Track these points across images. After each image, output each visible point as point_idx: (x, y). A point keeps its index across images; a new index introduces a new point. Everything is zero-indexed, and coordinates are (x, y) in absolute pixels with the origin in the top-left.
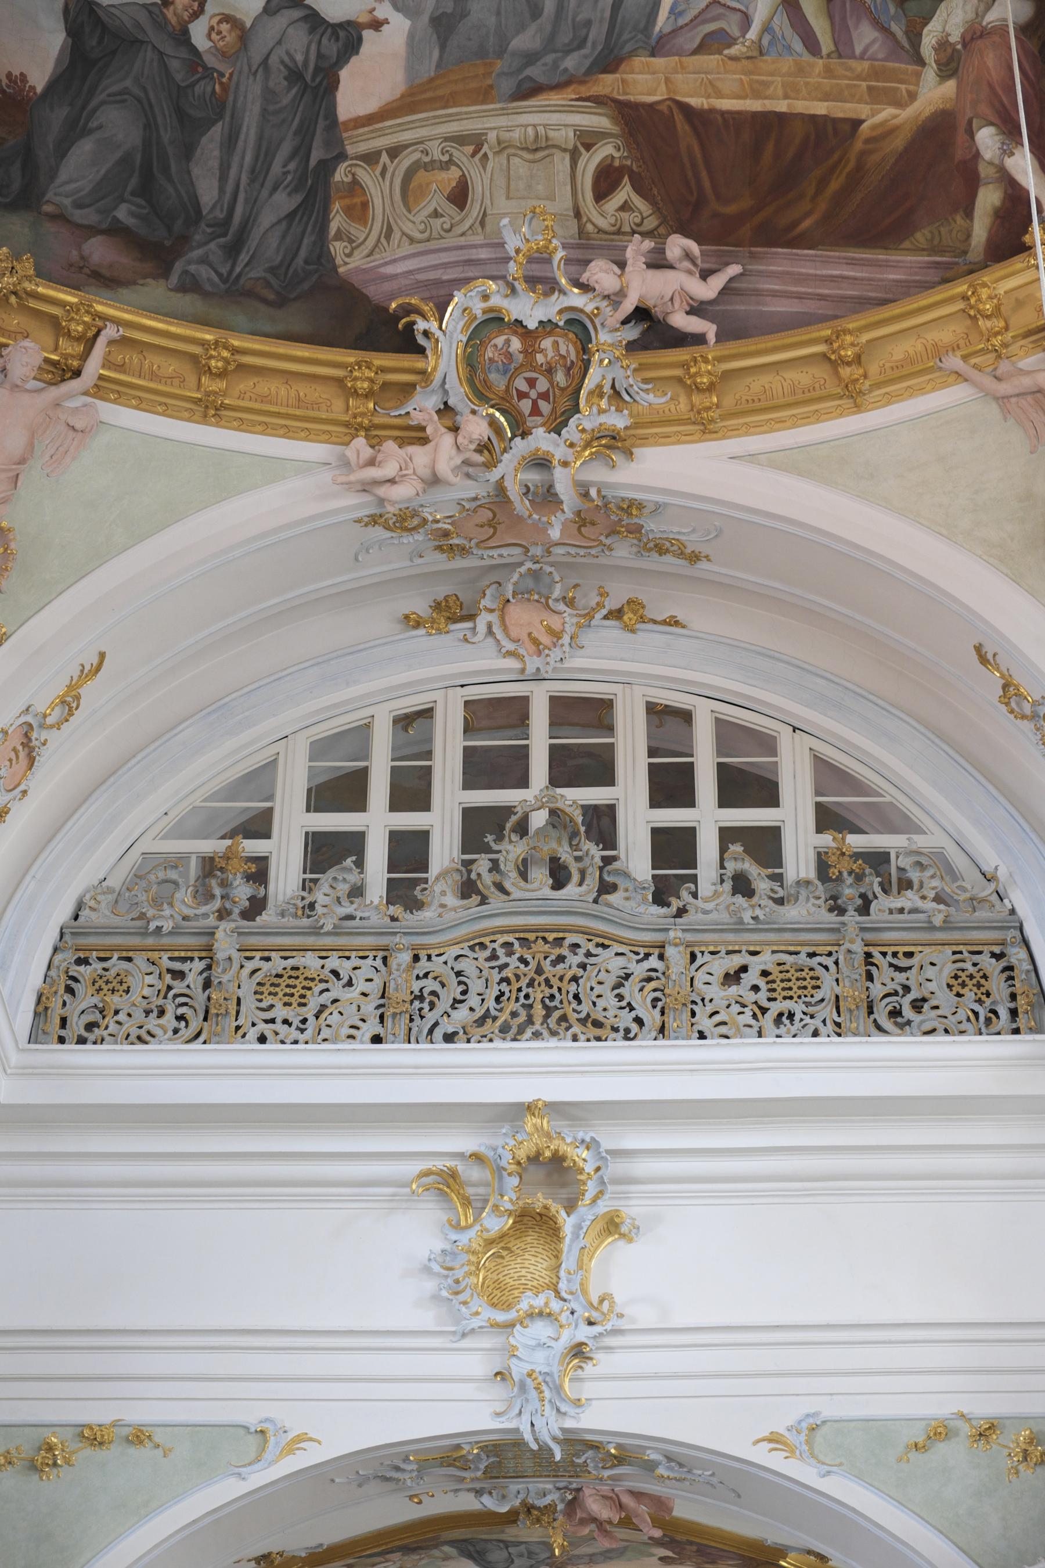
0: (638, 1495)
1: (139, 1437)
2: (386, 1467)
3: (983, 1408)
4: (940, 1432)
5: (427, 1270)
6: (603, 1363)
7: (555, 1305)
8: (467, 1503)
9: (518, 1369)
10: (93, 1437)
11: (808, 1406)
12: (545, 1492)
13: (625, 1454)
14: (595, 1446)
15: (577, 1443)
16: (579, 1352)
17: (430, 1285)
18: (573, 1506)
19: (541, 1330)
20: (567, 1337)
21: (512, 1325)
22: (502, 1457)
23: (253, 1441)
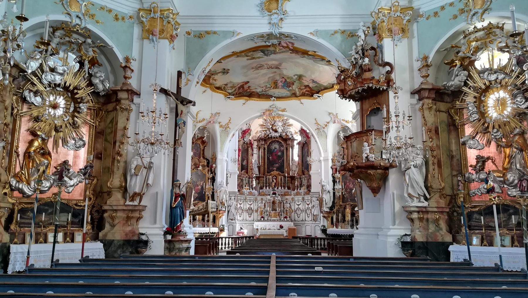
0: (289, 42)
1: (215, 33)
2: (252, 38)
3: (343, 28)
4: (336, 32)
5: (258, 6)
6: (285, 21)
7: (278, 12)
8: (264, 44)
9: (272, 22)
10: (208, 33)
11: (316, 28)
12: (275, 42)
13: (288, 36)
14: (283, 34)
15: (281, 34)
16: (281, 19)
17: (258, 8)
18: (279, 44)
19: (276, 16)
20: (280, 17)
21: (271, 15)
22: (270, 36)
23: (232, 33)
